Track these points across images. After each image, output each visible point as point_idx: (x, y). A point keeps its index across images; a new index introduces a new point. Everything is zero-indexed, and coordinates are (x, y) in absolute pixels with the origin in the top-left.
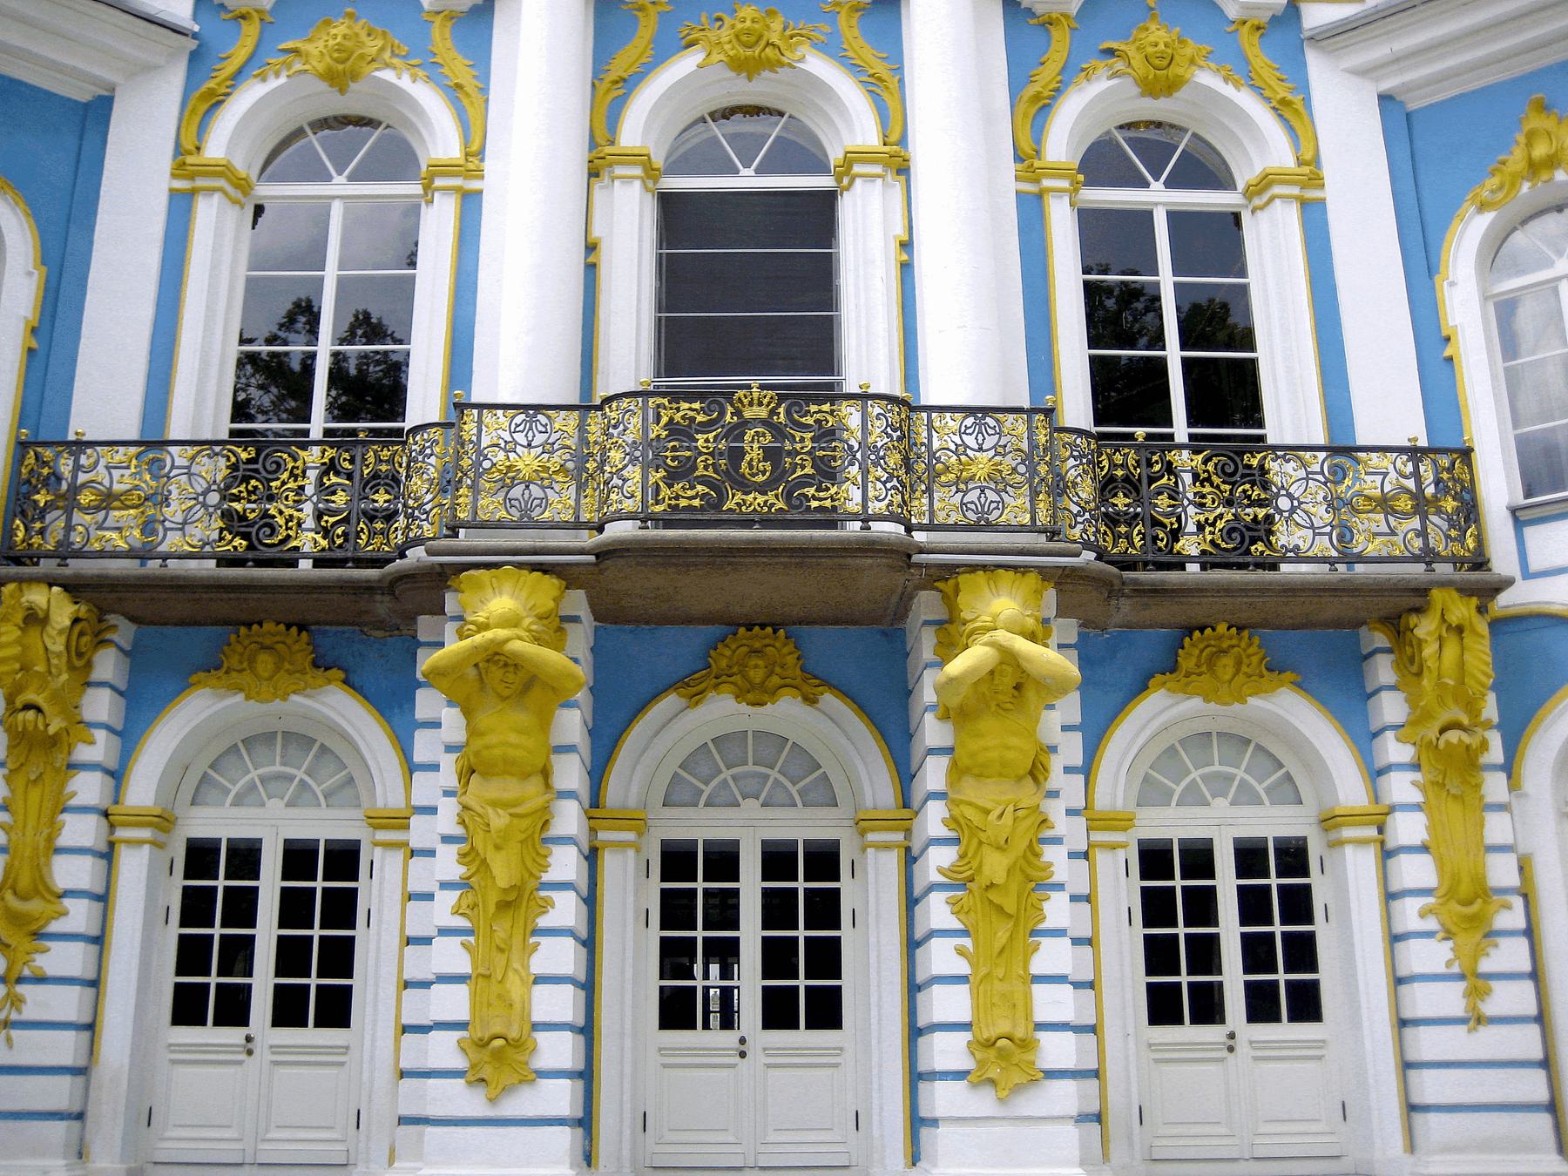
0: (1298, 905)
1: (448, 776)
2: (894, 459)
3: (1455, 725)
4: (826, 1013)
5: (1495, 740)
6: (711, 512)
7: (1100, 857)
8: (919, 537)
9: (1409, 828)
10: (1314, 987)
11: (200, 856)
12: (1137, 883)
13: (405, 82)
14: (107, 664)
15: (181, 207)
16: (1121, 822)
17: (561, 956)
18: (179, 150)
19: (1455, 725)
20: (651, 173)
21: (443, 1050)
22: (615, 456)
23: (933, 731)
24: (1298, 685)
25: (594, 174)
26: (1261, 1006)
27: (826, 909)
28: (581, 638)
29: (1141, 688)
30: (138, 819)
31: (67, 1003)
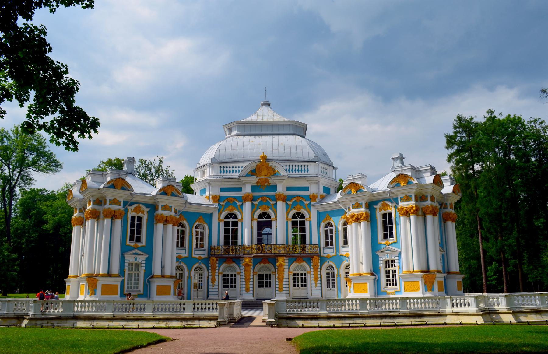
0: (305, 278)
1: (243, 271)
2: (273, 249)
4: (270, 286)
5: (319, 266)
6: (261, 253)
9: (312, 273)
10: (306, 284)
11: (224, 275)
12: (293, 277)
13: (236, 212)
15: (219, 223)
17: (251, 283)
21: (244, 289)
23: (277, 267)
24: (305, 262)
25: (252, 220)
26: (302, 286)
27: (270, 279)
28: (252, 261)
29: (293, 263)
30: (220, 273)
31: (217, 287)
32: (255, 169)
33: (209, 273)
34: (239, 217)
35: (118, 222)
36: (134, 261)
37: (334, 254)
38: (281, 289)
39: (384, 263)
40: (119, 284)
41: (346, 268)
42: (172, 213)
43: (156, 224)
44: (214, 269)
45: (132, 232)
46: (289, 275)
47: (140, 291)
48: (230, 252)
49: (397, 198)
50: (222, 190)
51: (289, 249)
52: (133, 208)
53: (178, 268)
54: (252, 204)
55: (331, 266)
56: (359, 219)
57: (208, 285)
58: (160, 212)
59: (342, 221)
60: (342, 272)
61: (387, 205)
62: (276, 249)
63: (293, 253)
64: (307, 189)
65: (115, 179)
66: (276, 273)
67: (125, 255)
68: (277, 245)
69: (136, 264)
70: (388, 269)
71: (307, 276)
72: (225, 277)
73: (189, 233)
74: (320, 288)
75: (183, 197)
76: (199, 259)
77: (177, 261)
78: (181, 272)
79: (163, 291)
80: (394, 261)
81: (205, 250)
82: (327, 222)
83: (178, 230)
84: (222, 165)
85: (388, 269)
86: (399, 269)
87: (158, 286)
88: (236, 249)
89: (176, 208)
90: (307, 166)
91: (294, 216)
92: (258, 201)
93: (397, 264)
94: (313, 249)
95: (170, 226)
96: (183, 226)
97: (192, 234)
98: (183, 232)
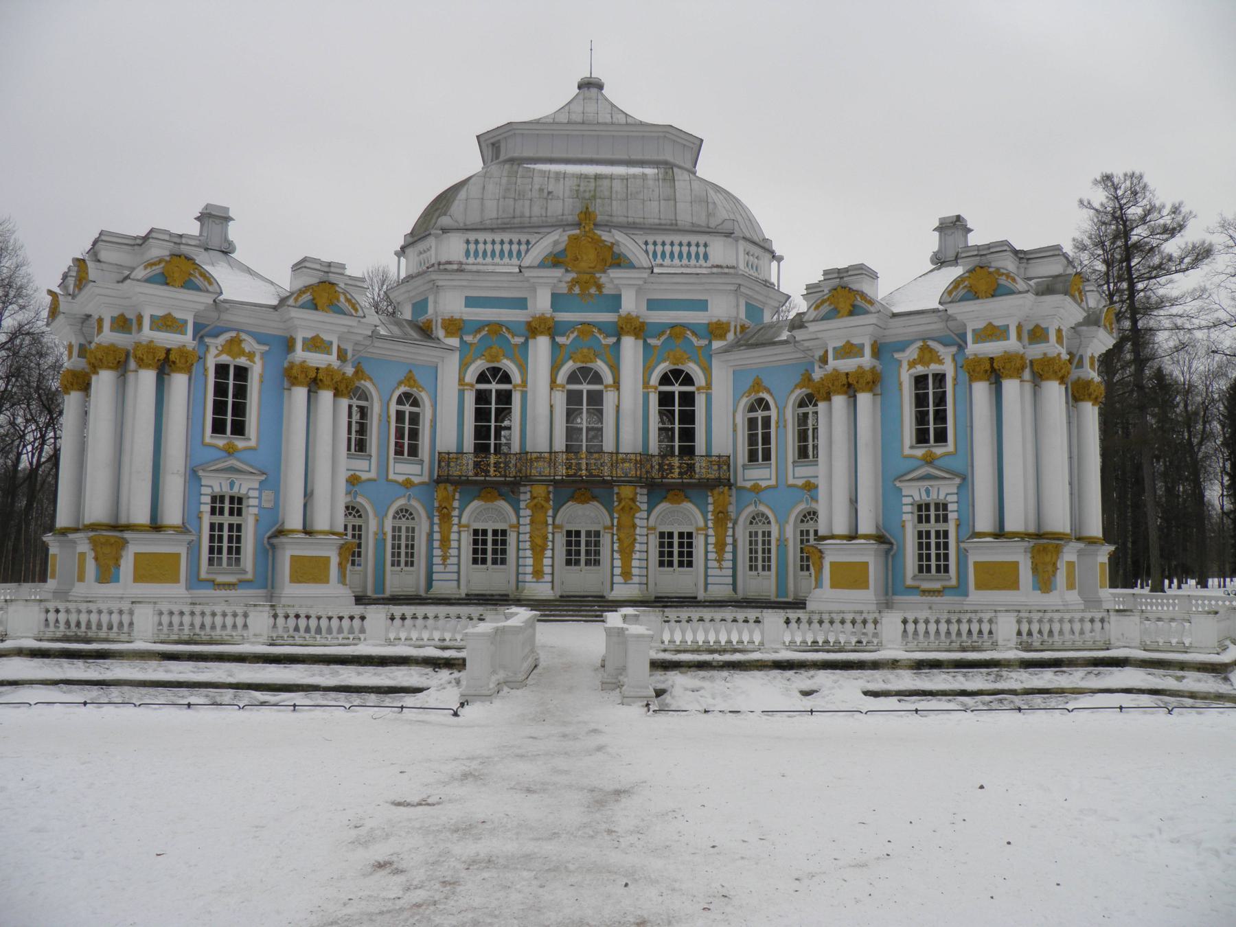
0: (690, 545)
1: (528, 520)
2: (609, 465)
3: (721, 512)
7: (650, 536)
8: (615, 479)
11: (476, 532)
12: (658, 540)
14: (457, 496)
15: (461, 393)
16: (654, 529)
18: (460, 380)
19: (721, 512)
20: (564, 387)
22: (557, 464)
23: (616, 515)
25: (552, 389)
26: (681, 564)
30: (464, 526)
32: (565, 250)
33: (432, 524)
34: (516, 377)
35: (179, 382)
36: (226, 490)
37: (773, 482)
38: (627, 575)
39: (916, 508)
40: (183, 551)
41: (802, 521)
42: (332, 359)
43: (290, 389)
44: (446, 518)
45: (219, 407)
46: (647, 535)
47: (245, 572)
48: (489, 471)
49: (963, 336)
50: (471, 302)
51: (652, 467)
52: (223, 343)
53: (351, 510)
54: (554, 344)
55: (763, 515)
56: (849, 385)
57: (430, 557)
58: (300, 354)
59: (799, 393)
60: (790, 532)
61: (931, 350)
62: (614, 465)
63: (663, 477)
64: (702, 305)
65: (168, 259)
66: (615, 528)
67: (201, 473)
68: (617, 453)
69: (232, 499)
70: (924, 527)
71: (694, 541)
72: (479, 536)
73: (380, 415)
74: (730, 572)
75: (365, 317)
76: (408, 484)
77: (348, 493)
78: (357, 522)
79: (309, 571)
80: (945, 506)
81: (421, 462)
82: (754, 397)
83: (350, 407)
84: (472, 236)
85: (924, 527)
86: (958, 526)
87: (292, 557)
88: (507, 464)
89: (342, 346)
90: (706, 245)
91: (665, 380)
92: (572, 336)
93: (952, 516)
94: (716, 467)
95: (326, 396)
96: (364, 396)
97: (389, 417)
98: (363, 412)
